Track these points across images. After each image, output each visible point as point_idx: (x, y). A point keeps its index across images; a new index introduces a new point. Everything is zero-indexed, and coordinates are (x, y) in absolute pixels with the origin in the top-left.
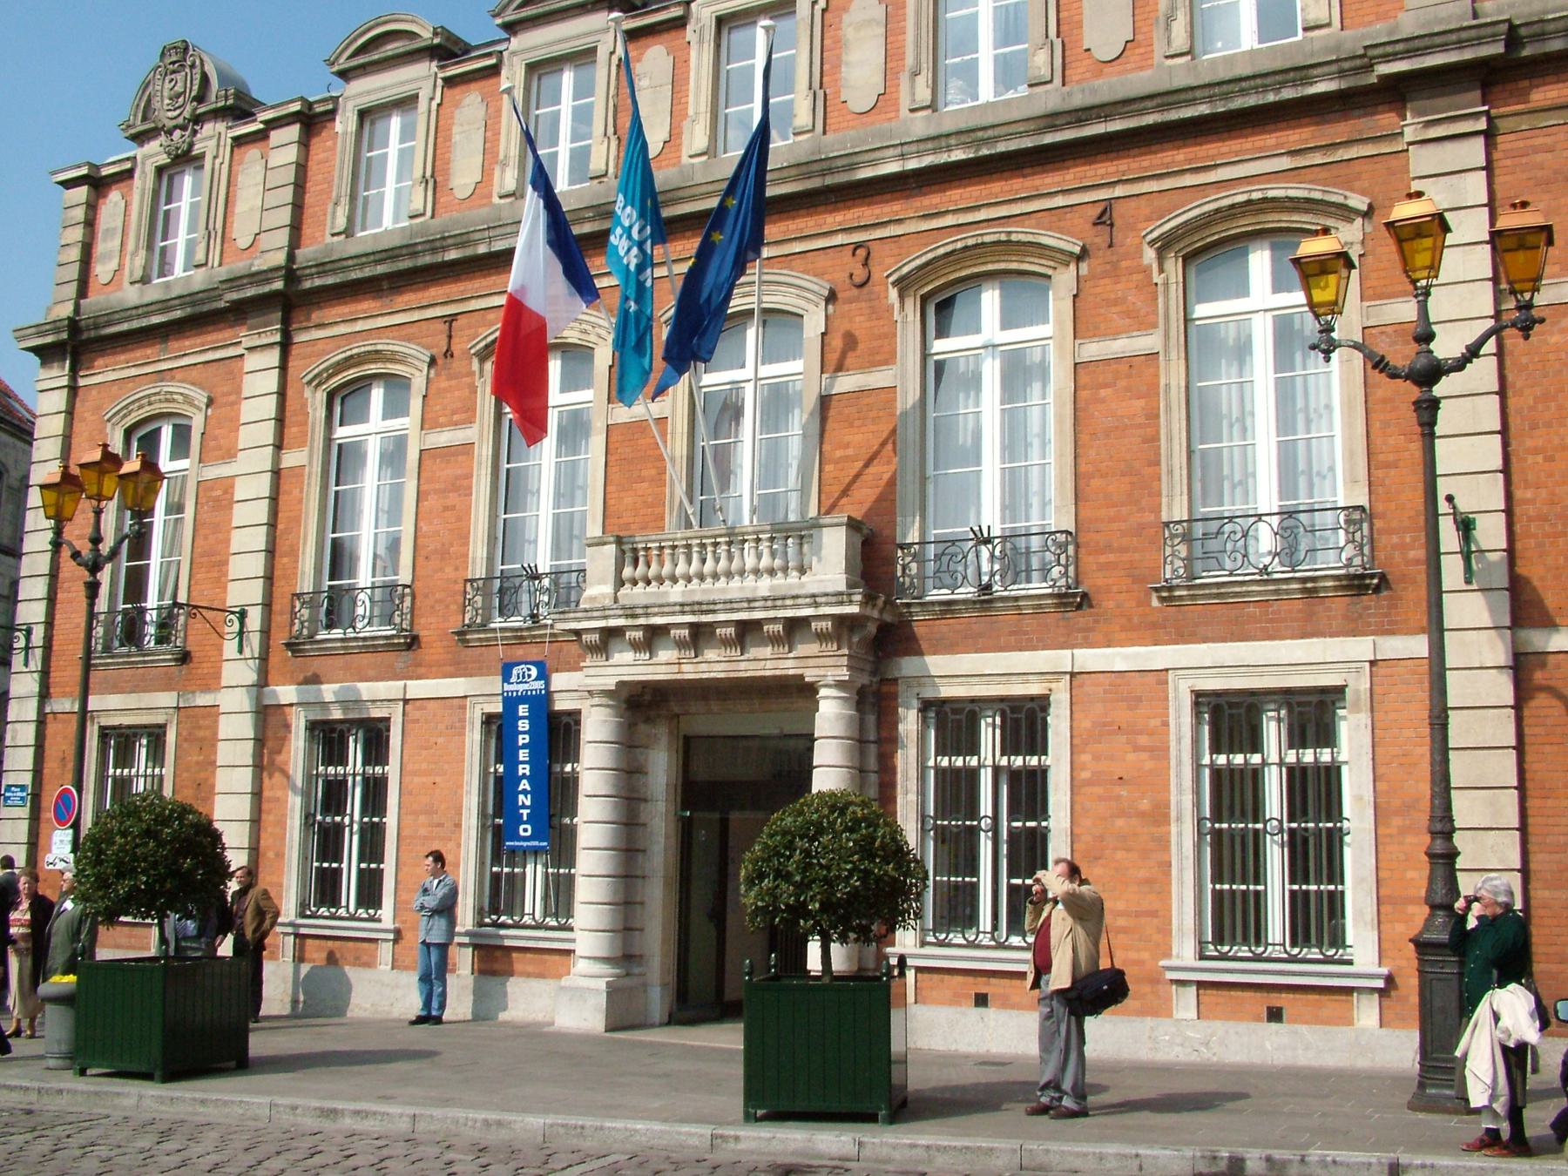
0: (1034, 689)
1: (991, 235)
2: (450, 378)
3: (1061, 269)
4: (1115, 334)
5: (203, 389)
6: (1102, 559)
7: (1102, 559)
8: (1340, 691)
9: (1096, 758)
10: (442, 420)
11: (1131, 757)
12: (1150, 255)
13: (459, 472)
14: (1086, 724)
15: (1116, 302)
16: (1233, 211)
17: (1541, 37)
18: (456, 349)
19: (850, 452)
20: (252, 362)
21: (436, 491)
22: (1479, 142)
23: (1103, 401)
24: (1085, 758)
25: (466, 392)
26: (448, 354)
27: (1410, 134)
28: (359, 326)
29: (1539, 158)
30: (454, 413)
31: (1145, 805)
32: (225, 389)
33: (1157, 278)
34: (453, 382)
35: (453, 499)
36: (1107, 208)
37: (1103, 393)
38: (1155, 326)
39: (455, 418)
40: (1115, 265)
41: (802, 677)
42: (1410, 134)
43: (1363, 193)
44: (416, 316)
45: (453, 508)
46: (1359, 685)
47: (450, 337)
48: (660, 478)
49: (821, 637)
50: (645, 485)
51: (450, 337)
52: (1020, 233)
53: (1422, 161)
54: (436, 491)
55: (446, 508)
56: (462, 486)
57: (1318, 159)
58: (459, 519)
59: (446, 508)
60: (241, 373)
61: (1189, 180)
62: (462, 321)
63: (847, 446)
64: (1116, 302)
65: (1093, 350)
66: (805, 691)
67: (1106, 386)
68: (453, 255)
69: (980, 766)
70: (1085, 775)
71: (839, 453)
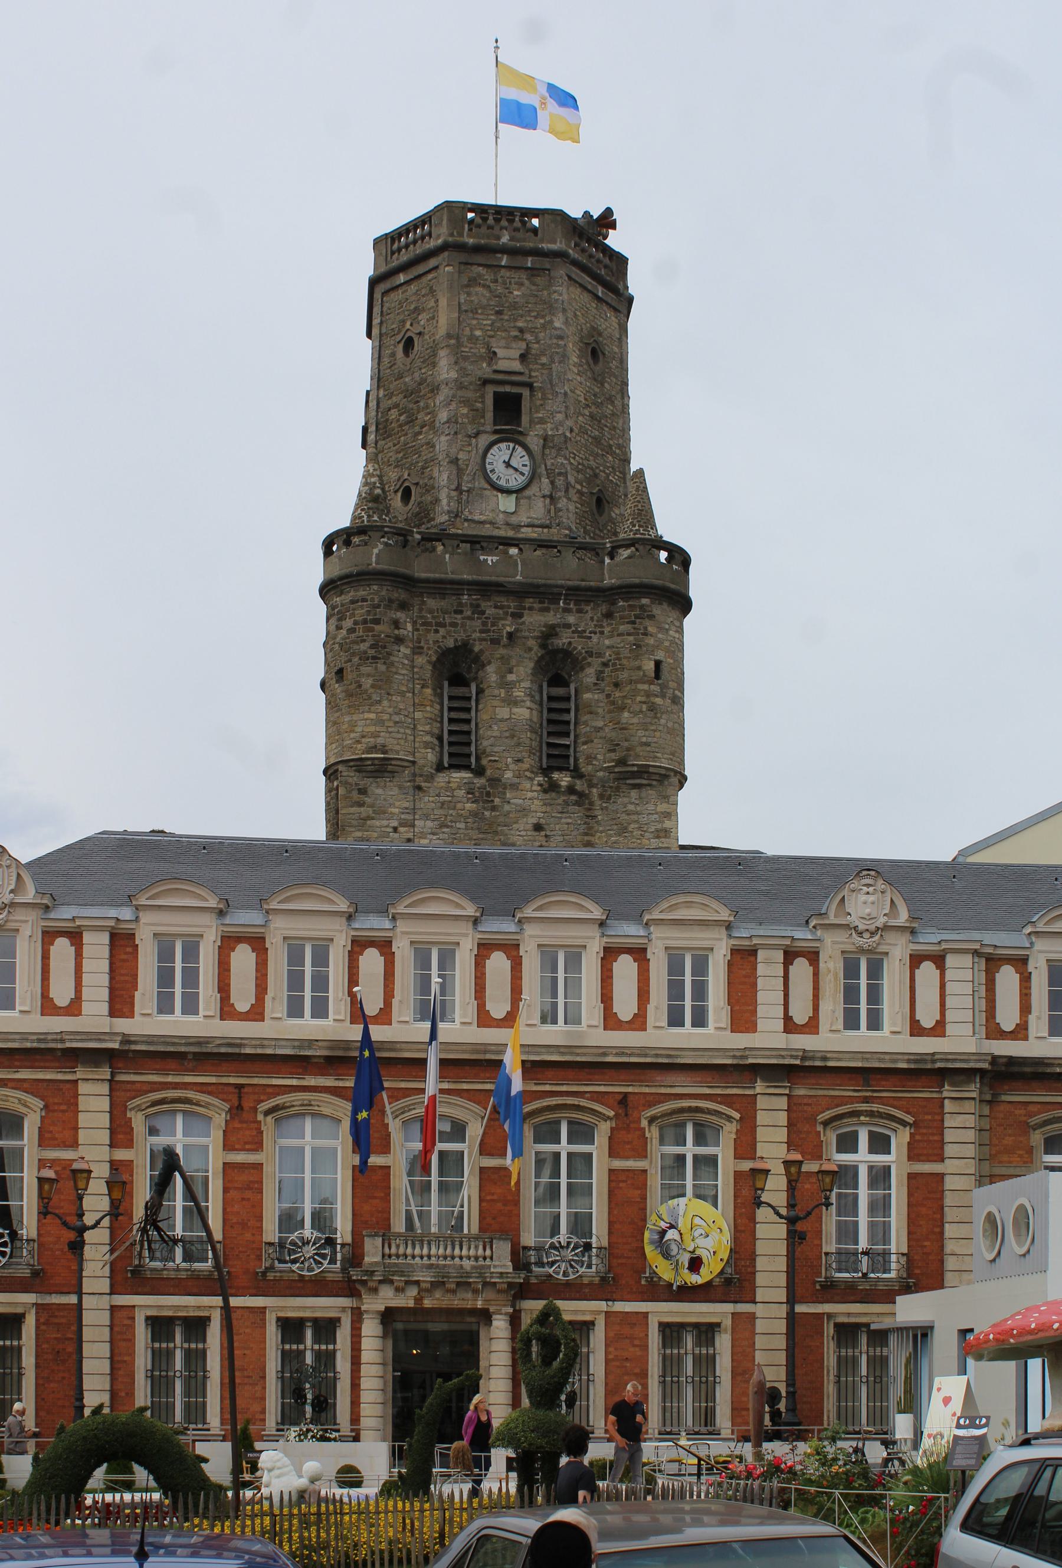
0: (588, 1318)
1: (570, 1101)
2: (241, 1122)
3: (603, 1122)
4: (627, 1158)
5: (43, 1100)
6: (620, 1261)
7: (620, 1261)
8: (718, 1325)
9: (616, 1349)
10: (237, 1146)
11: (632, 1349)
12: (644, 1123)
13: (252, 1179)
14: (611, 1334)
15: (628, 1143)
16: (682, 1110)
17: (813, 1058)
18: (247, 1104)
19: (495, 1197)
20: (83, 1088)
21: (236, 1188)
22: (785, 1098)
23: (621, 1188)
24: (611, 1349)
25: (254, 1133)
26: (240, 1107)
27: (758, 1090)
28: (170, 1079)
29: (805, 1108)
30: (246, 1143)
31: (637, 1370)
32: (56, 1101)
33: (647, 1135)
34: (245, 1125)
35: (248, 1194)
36: (626, 1094)
37: (621, 1185)
38: (646, 1157)
39: (247, 1147)
40: (628, 1125)
41: (488, 1309)
42: (758, 1090)
43: (736, 1110)
44: (213, 1080)
45: (249, 1199)
46: (727, 1322)
47: (240, 1098)
48: (387, 1198)
49: (499, 1291)
50: (377, 1201)
51: (240, 1098)
52: (583, 1102)
53: (761, 1103)
54: (236, 1188)
55: (243, 1199)
56: (256, 1186)
57: (719, 1091)
58: (253, 1206)
59: (243, 1199)
60: (76, 1096)
61: (663, 1090)
62: (246, 1090)
63: (493, 1194)
64: (628, 1143)
65: (618, 1164)
66: (486, 1316)
67: (623, 1181)
68: (248, 1051)
69: (175, 1347)
70: (611, 1357)
71: (488, 1198)
